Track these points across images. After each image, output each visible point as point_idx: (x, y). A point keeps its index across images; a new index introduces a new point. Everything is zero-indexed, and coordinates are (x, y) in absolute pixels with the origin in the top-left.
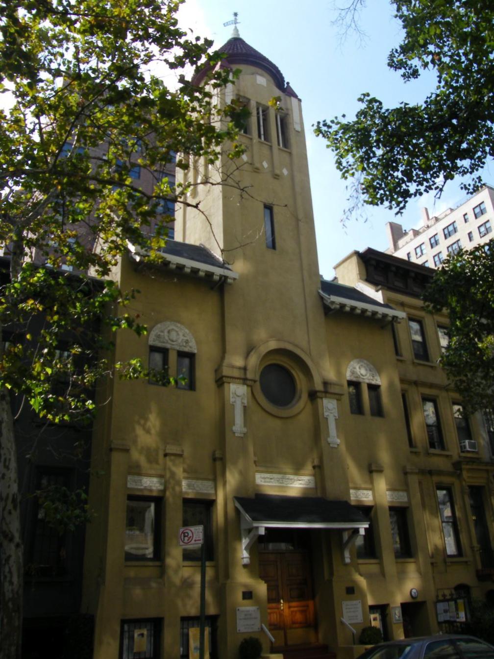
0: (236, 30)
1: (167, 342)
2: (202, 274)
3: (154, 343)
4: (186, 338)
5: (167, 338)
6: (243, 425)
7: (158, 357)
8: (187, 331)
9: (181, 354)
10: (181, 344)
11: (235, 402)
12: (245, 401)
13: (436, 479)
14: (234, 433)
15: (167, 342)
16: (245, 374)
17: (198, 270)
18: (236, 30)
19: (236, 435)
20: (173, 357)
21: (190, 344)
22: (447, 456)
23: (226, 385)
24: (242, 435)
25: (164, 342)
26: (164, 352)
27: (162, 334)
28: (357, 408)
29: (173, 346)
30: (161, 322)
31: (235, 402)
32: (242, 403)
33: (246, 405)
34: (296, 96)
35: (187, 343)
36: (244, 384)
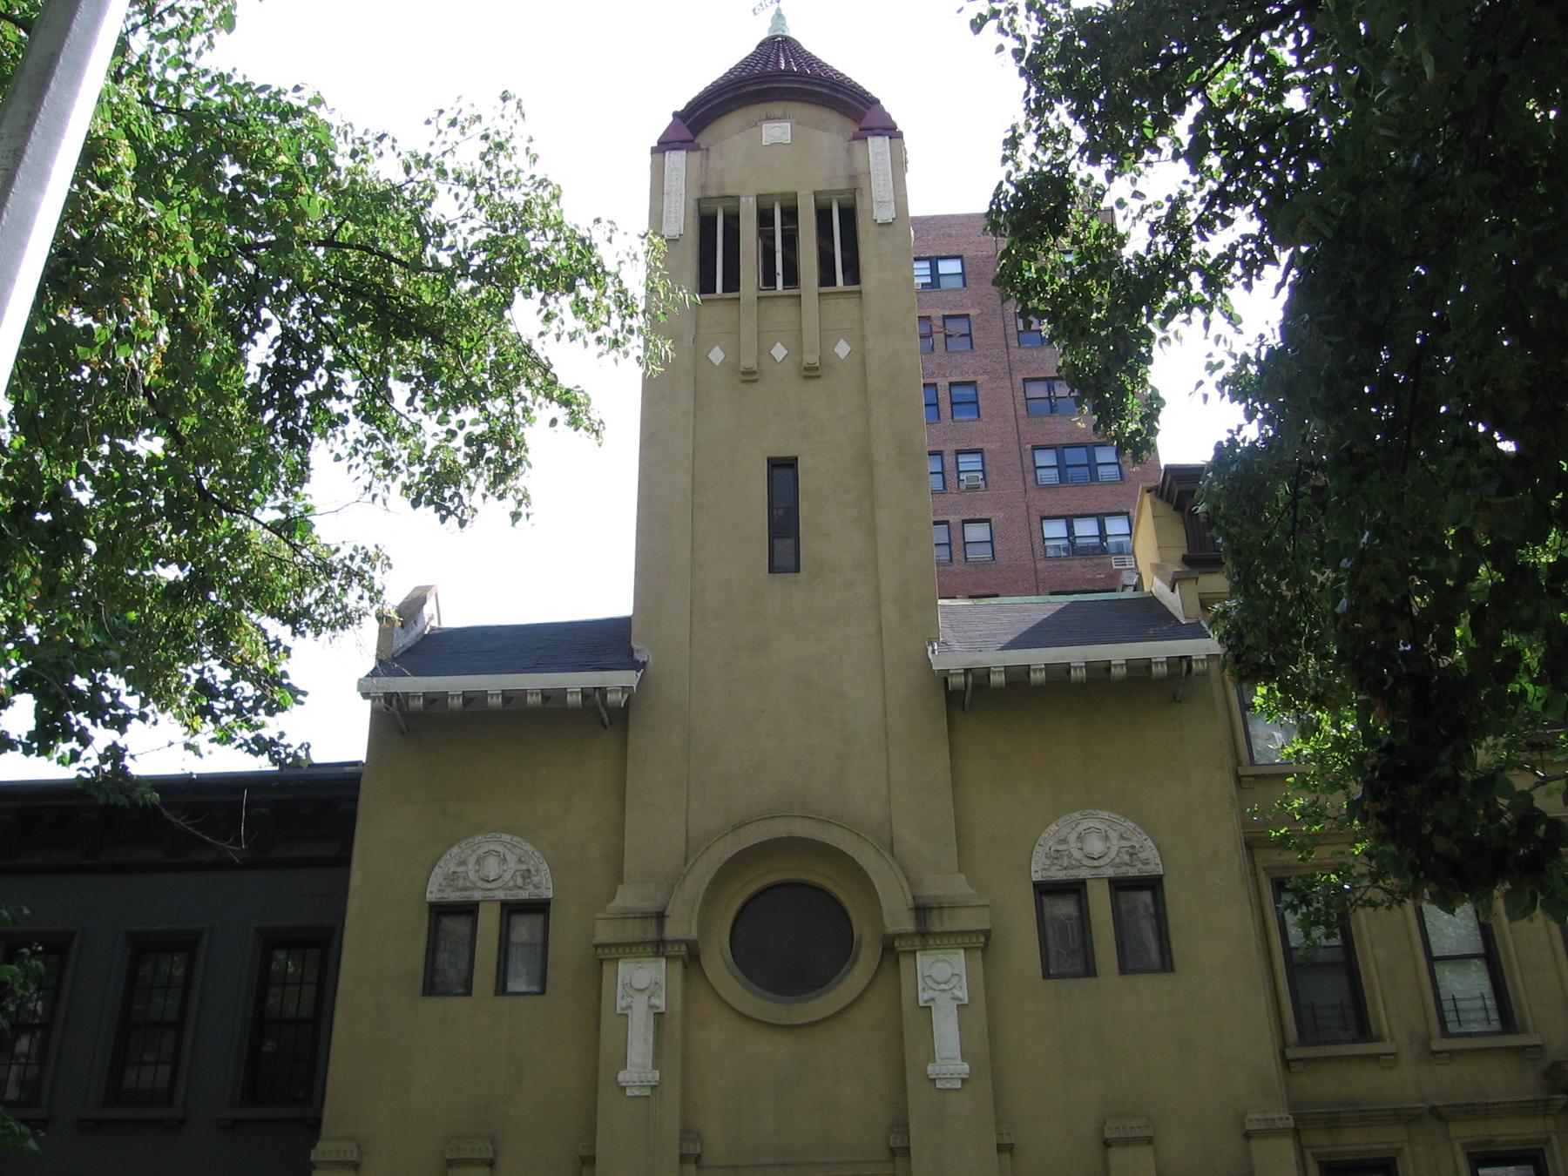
0: (779, 16)
1: (475, 887)
2: (997, 679)
3: (1045, 874)
4: (524, 867)
5: (1077, 854)
6: (650, 1062)
7: (1064, 908)
8: (528, 847)
9: (1119, 886)
10: (1118, 860)
11: (629, 1007)
12: (660, 1002)
13: (1467, 1132)
14: (624, 1088)
15: (475, 887)
16: (661, 927)
17: (1027, 670)
18: (779, 16)
19: (629, 1093)
20: (1100, 899)
21: (536, 879)
22: (1520, 1050)
23: (904, 962)
24: (647, 1092)
25: (466, 889)
26: (1075, 889)
27: (462, 869)
28: (1068, 956)
29: (1100, 871)
30: (459, 840)
31: (629, 1007)
32: (651, 1007)
33: (663, 1009)
34: (890, 130)
35: (1131, 855)
36: (657, 955)
